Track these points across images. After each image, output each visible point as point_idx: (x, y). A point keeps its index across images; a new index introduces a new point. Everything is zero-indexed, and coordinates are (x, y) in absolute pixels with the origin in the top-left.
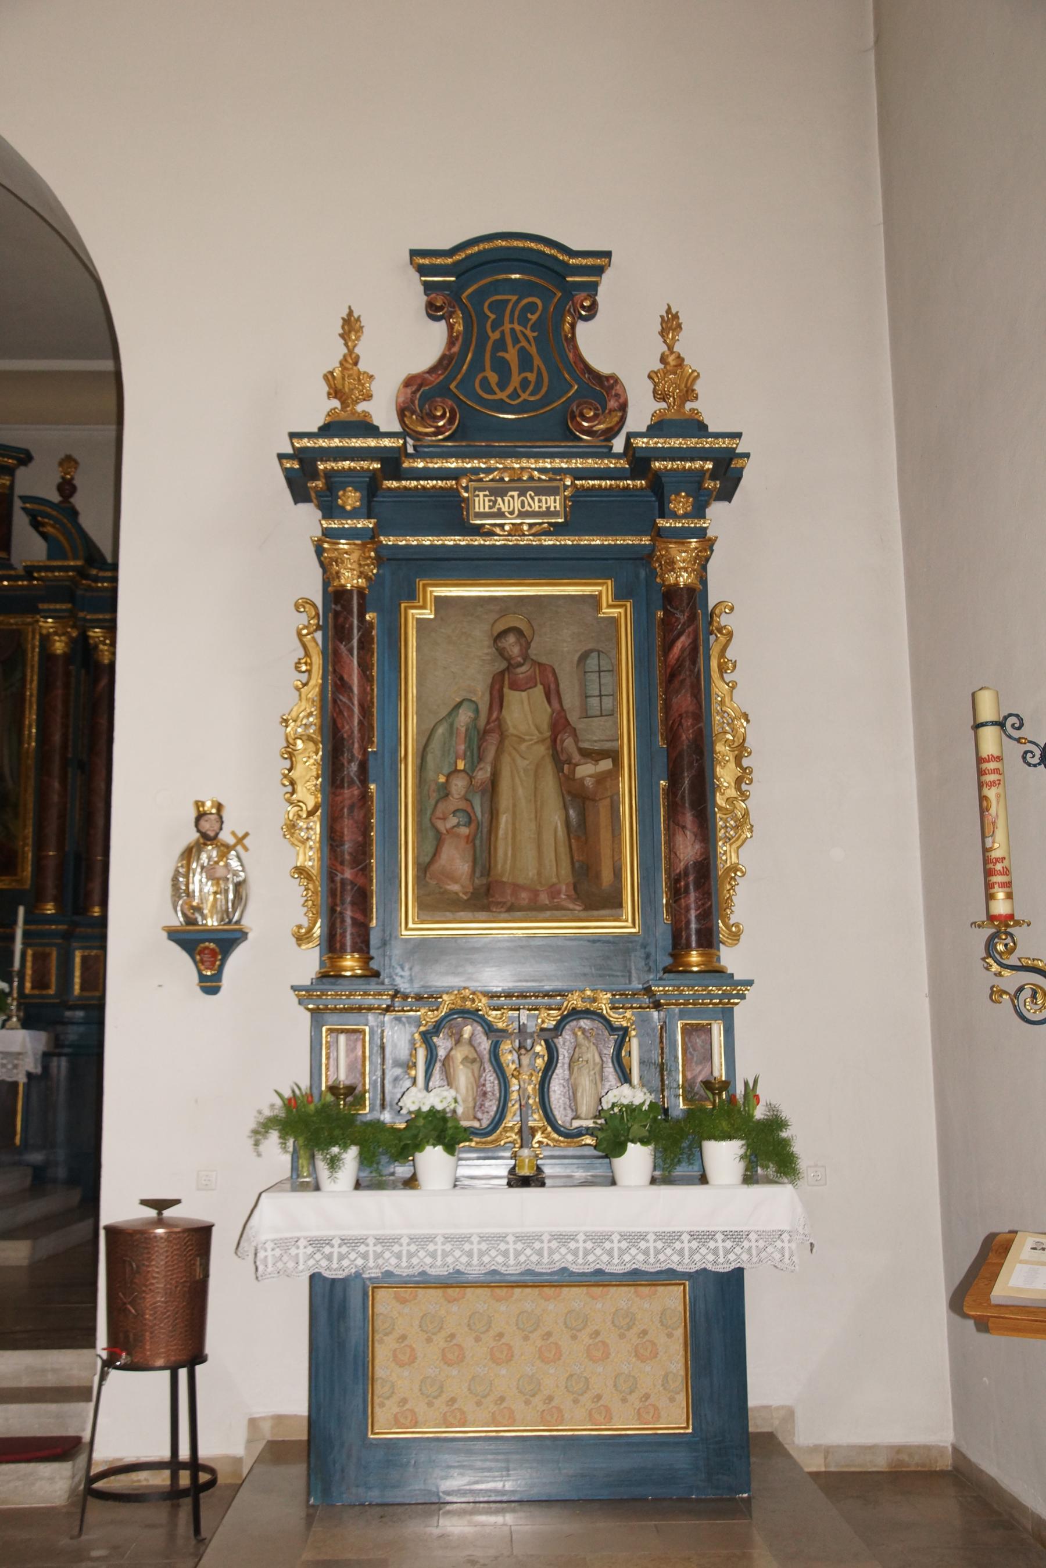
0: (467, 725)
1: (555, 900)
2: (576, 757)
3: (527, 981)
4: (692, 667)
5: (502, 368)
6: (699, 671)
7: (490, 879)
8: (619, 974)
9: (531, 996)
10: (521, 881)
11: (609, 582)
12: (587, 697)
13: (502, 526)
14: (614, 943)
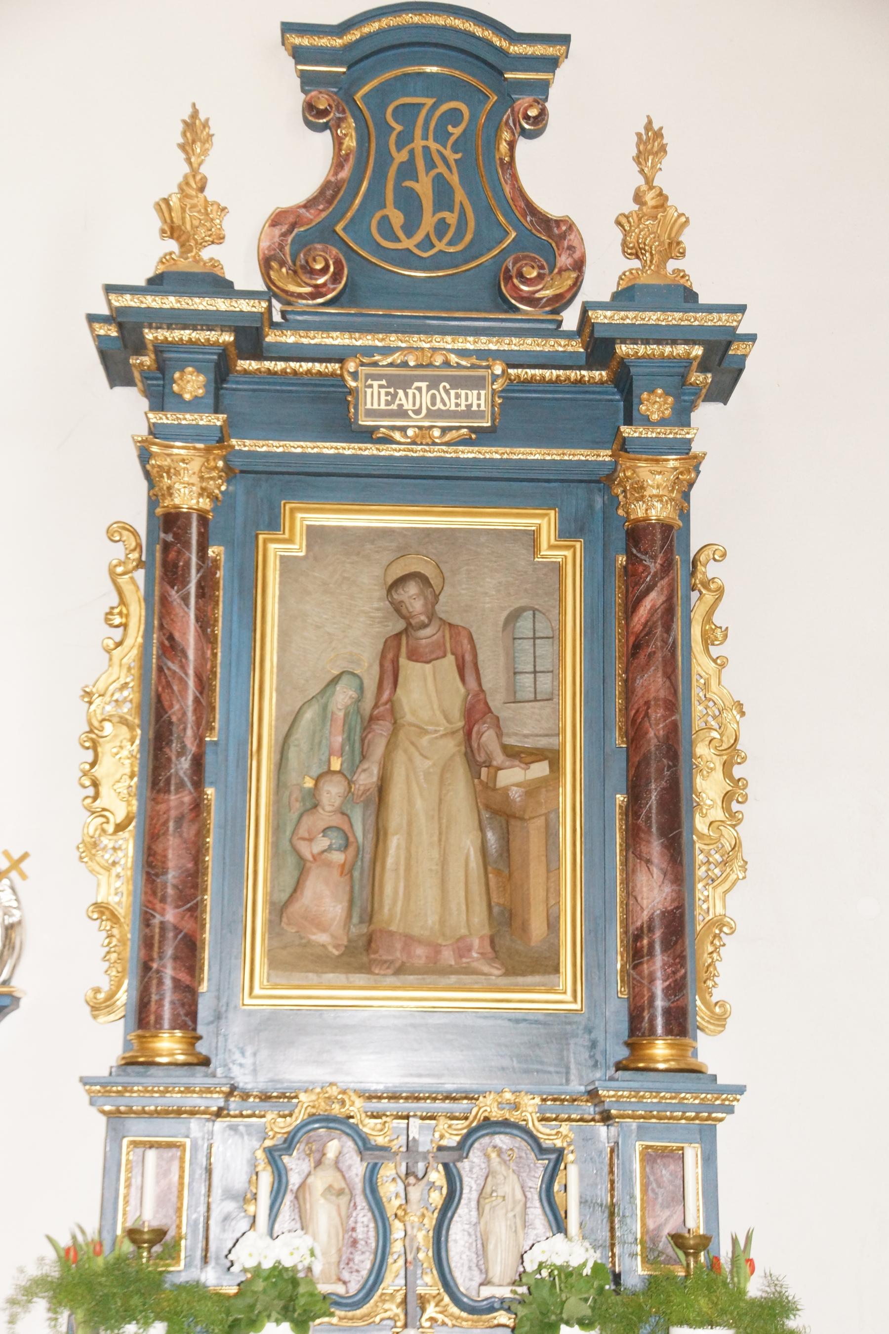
0: (347, 708)
1: (464, 960)
2: (499, 758)
3: (420, 1076)
4: (665, 635)
6: (674, 643)
7: (372, 927)
8: (552, 1069)
9: (425, 1099)
10: (416, 931)
11: (552, 513)
12: (515, 673)
13: (403, 429)
14: (545, 1024)
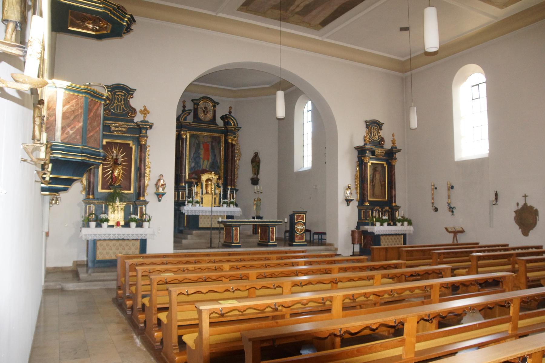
5: (374, 135)
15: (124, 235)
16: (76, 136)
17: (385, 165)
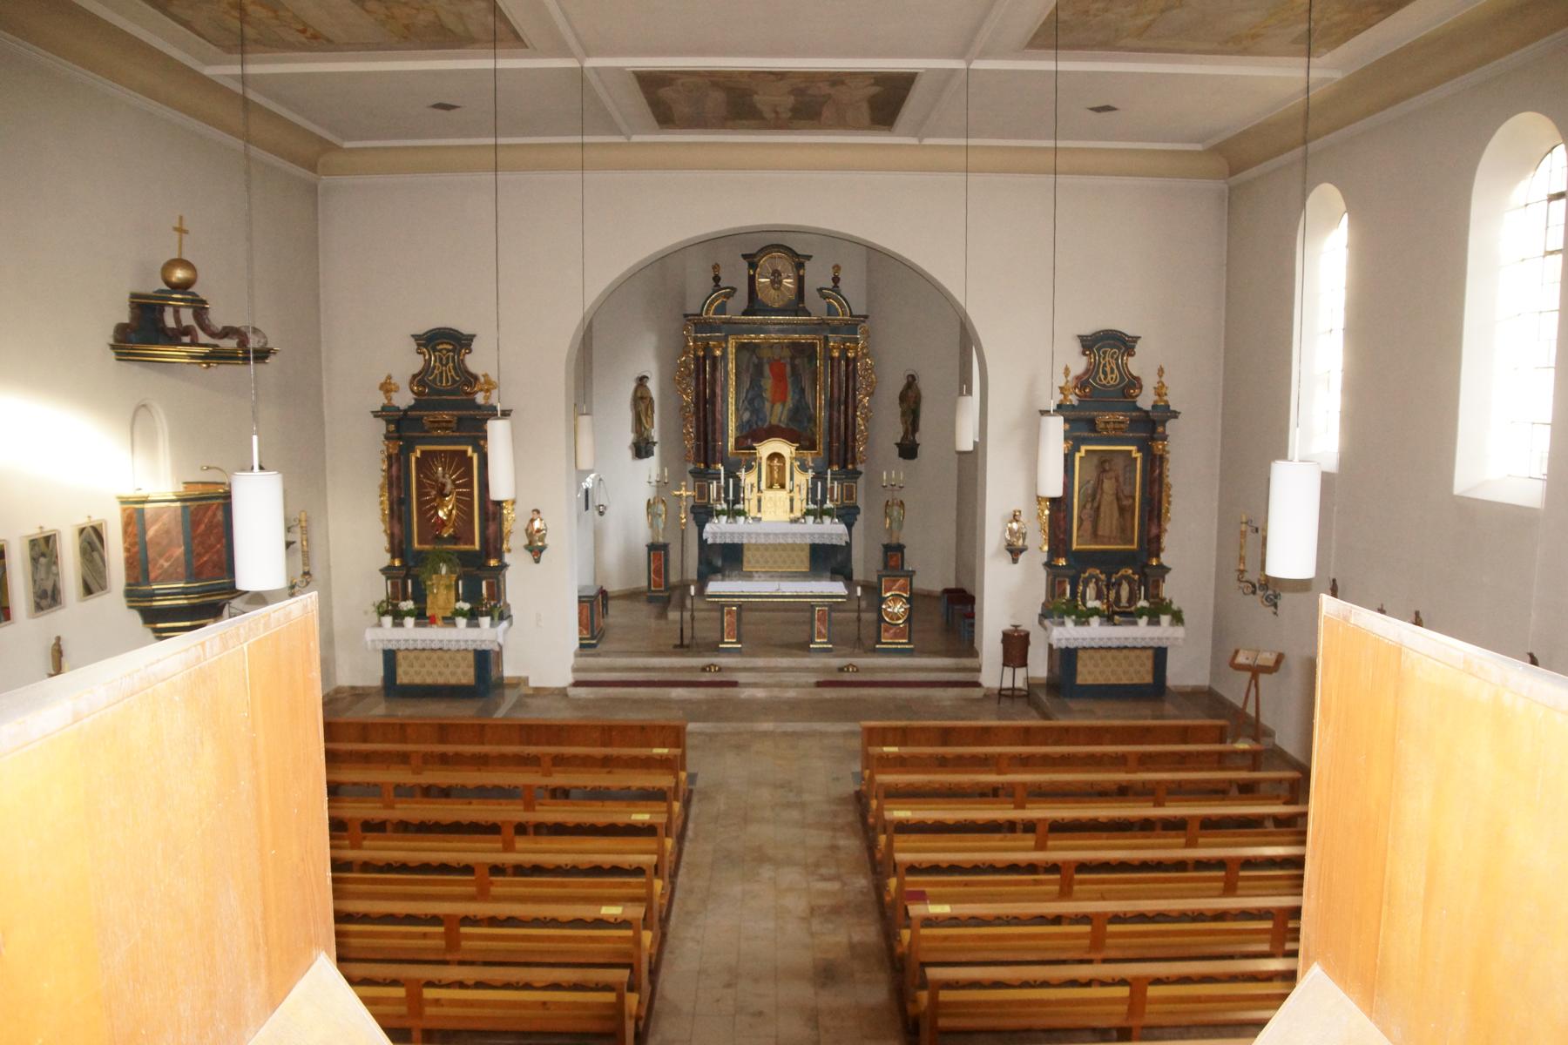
5: (1105, 373)
15: (441, 641)
16: (176, 569)
17: (1134, 455)
